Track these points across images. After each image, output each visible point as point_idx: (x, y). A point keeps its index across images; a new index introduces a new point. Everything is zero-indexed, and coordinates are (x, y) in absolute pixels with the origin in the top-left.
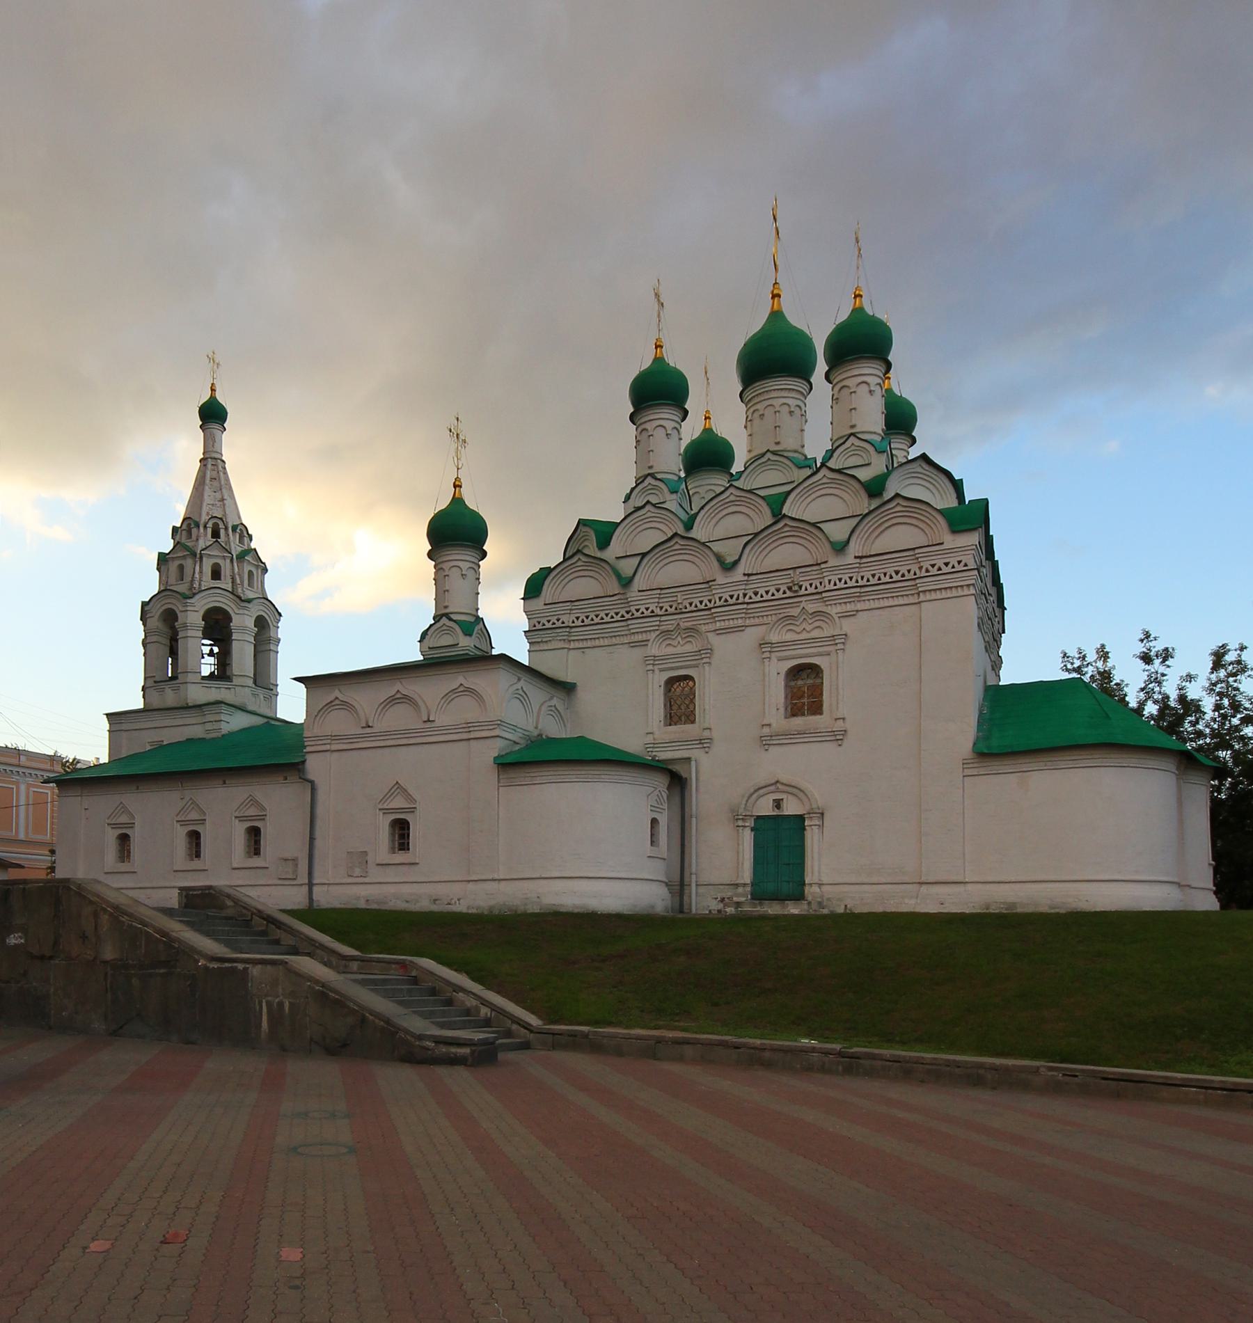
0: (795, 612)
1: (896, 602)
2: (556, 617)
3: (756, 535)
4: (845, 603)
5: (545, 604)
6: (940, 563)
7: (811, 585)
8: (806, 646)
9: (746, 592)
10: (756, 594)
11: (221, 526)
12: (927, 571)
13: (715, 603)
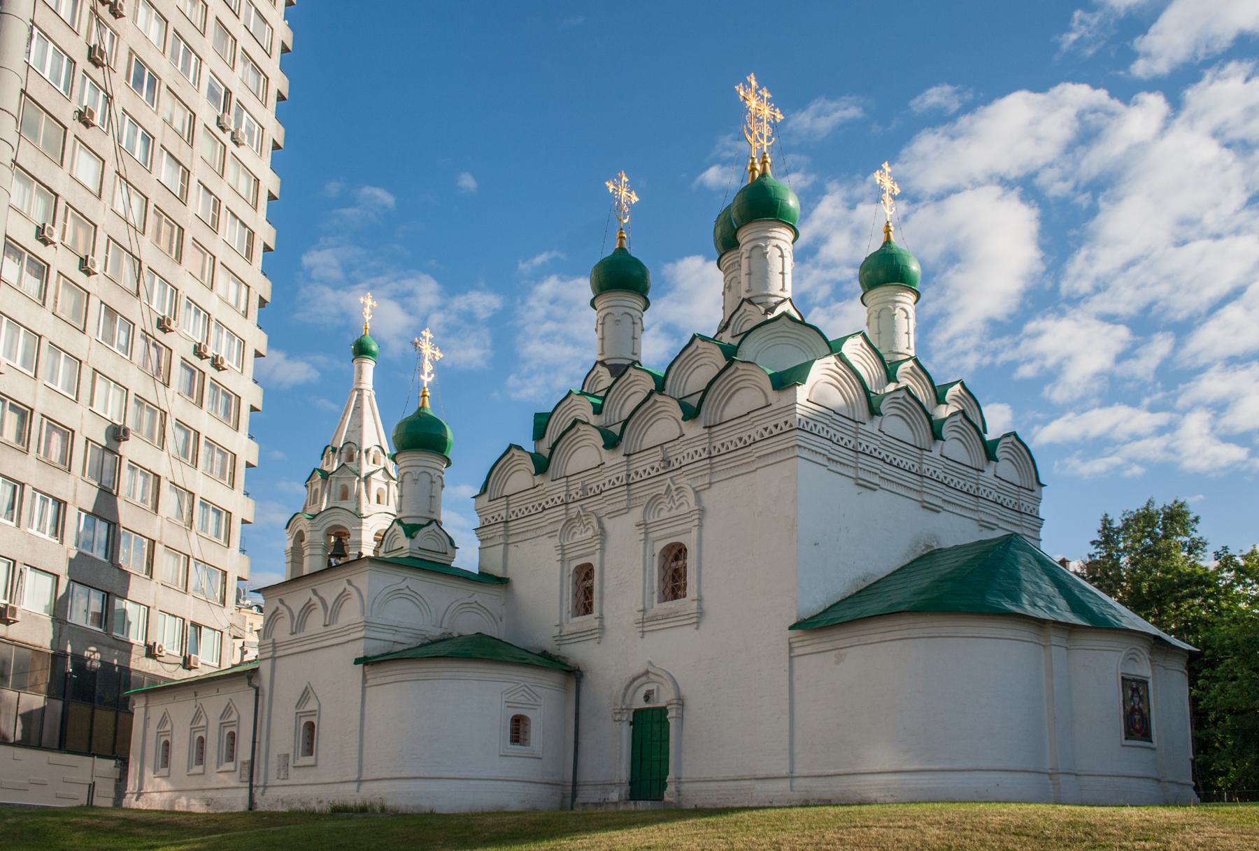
2: (497, 513)
5: (490, 501)
8: (685, 521)
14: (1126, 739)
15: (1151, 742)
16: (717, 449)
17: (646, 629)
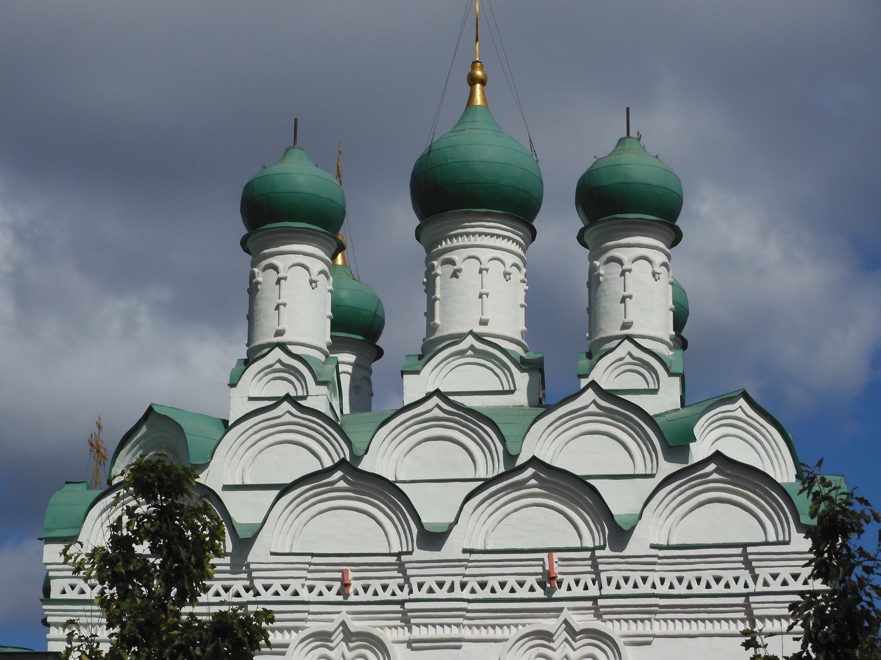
0: (549, 624)
1: (717, 628)
3: (487, 483)
4: (635, 621)
7: (577, 582)
9: (465, 579)
10: (483, 585)
12: (766, 584)
13: (411, 592)
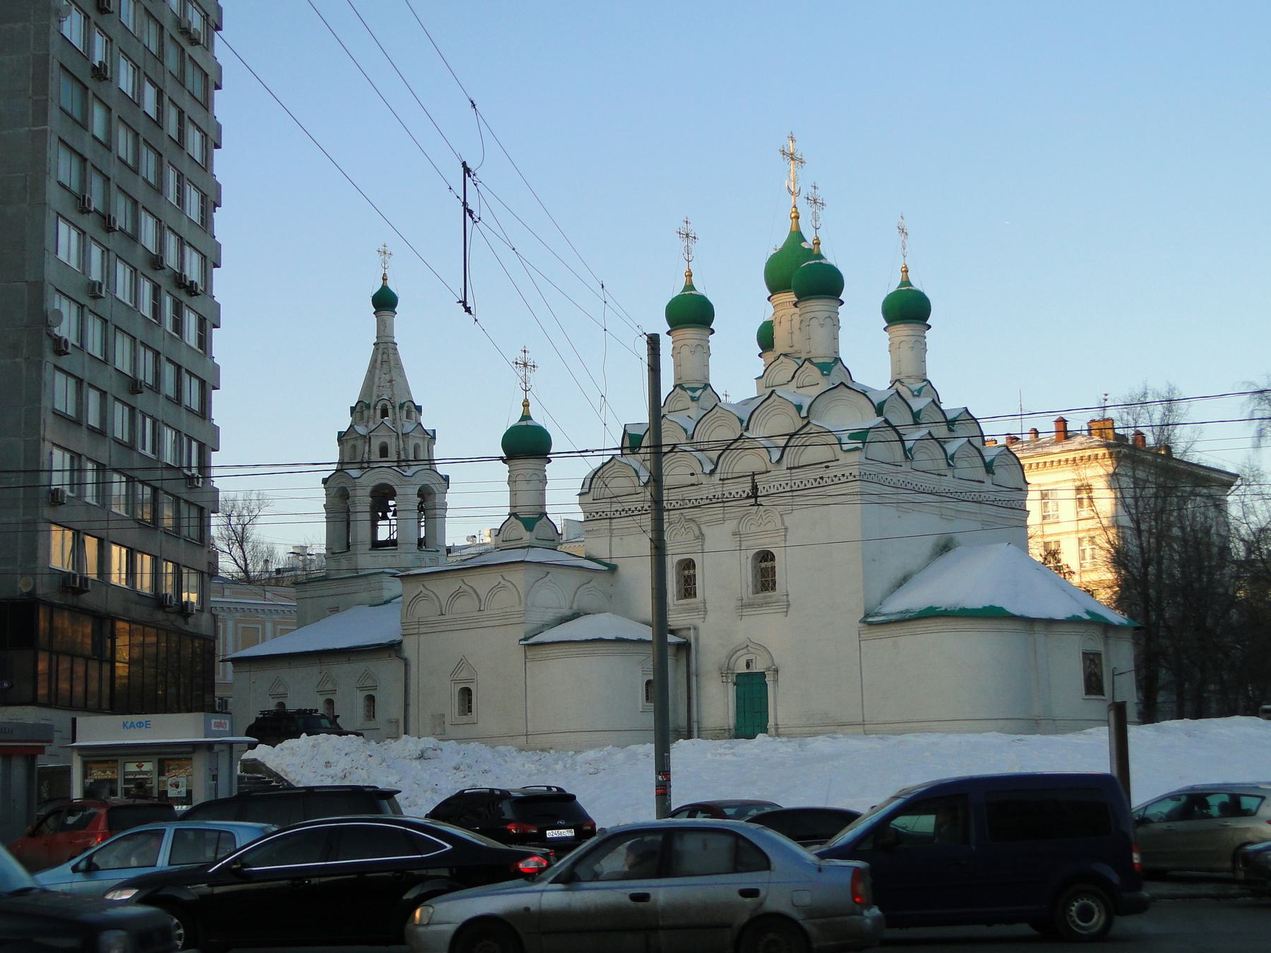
5: (593, 500)
6: (839, 475)
11: (389, 407)
14: (1086, 694)
15: (1103, 695)
16: (797, 485)
17: (743, 614)
